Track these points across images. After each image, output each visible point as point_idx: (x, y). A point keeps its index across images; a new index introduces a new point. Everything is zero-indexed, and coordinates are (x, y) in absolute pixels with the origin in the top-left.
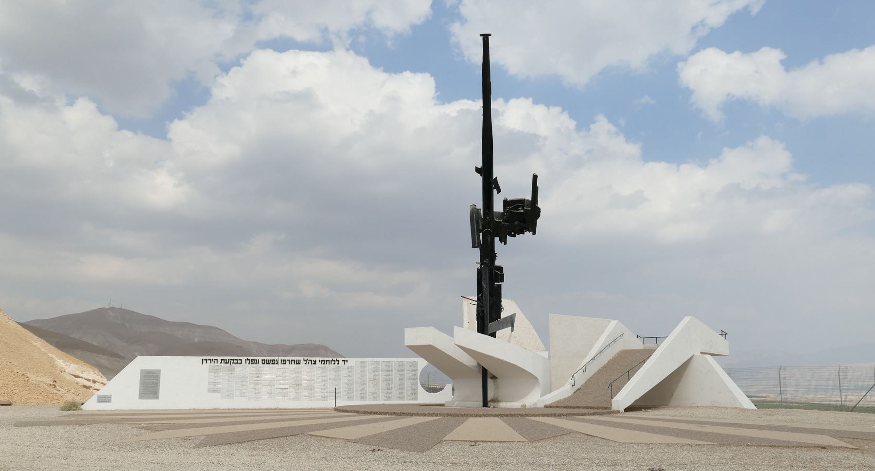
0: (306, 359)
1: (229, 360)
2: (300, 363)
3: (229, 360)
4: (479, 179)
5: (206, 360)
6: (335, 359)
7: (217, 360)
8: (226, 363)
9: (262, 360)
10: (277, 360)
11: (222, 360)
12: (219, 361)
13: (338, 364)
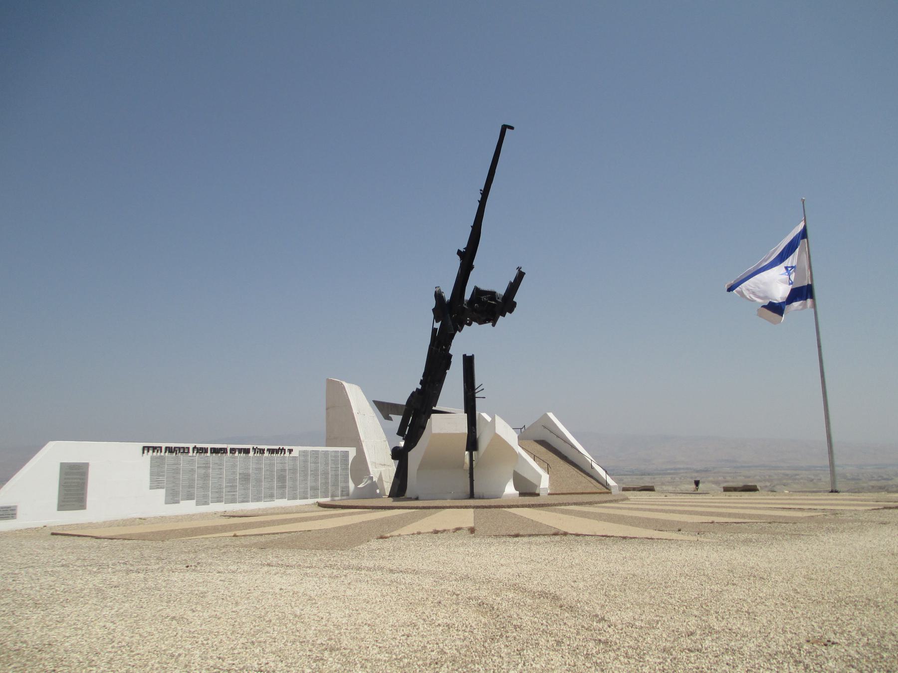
4: (457, 262)
13: (285, 453)
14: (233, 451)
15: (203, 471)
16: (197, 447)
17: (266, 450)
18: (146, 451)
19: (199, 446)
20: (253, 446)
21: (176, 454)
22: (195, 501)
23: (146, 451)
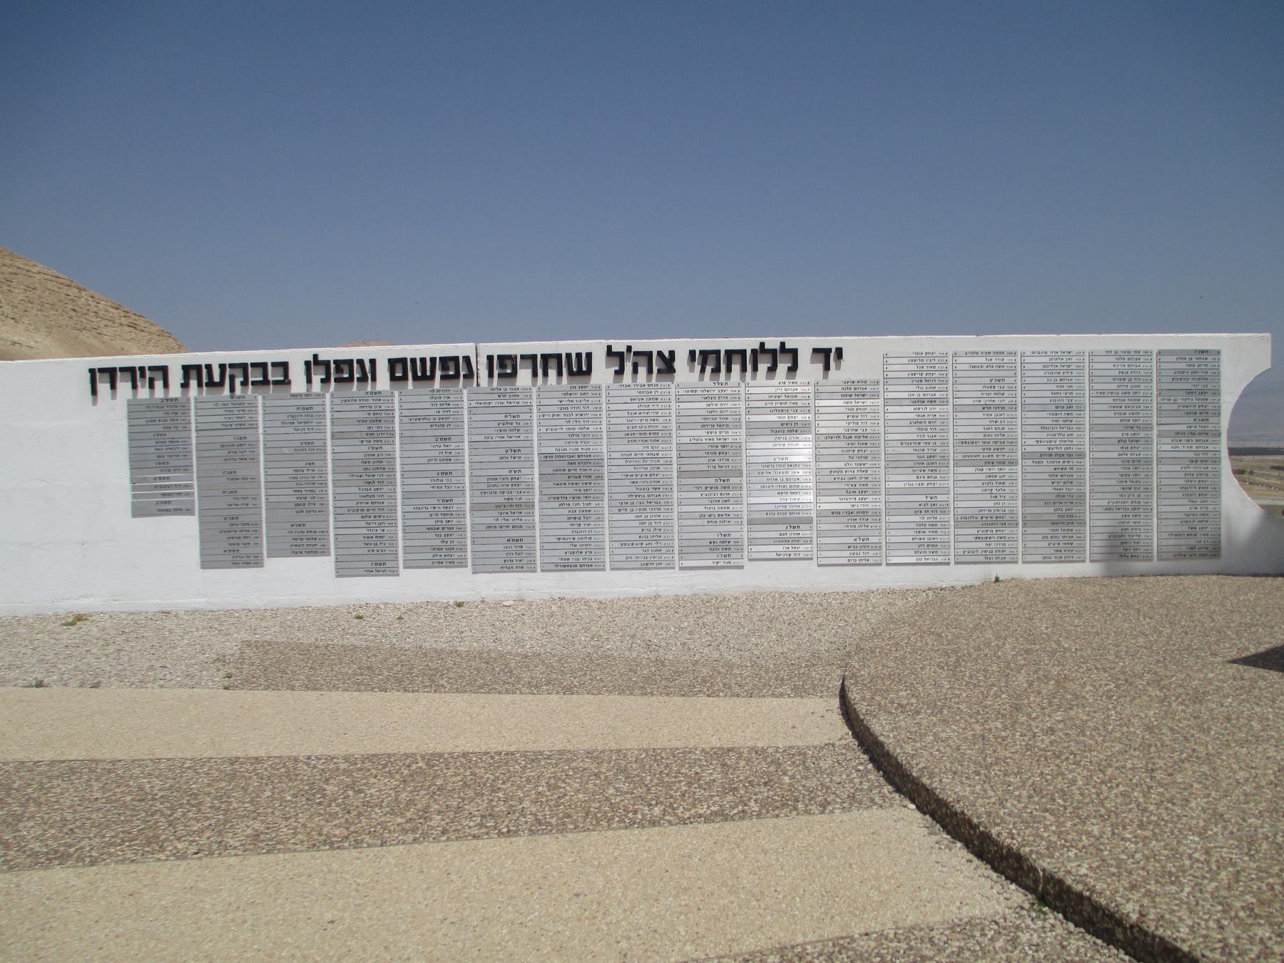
0: (620, 346)
1: (222, 367)
2: (589, 372)
3: (222, 367)
5: (111, 373)
6: (772, 343)
7: (164, 370)
8: (211, 384)
9: (393, 363)
10: (467, 359)
11: (187, 369)
12: (176, 377)
13: (793, 368)
14: (505, 366)
15: (358, 450)
16: (321, 358)
17: (833, 350)
18: (104, 387)
19: (330, 353)
20: (782, 339)
21: (232, 389)
22: (332, 558)
23: (104, 387)
